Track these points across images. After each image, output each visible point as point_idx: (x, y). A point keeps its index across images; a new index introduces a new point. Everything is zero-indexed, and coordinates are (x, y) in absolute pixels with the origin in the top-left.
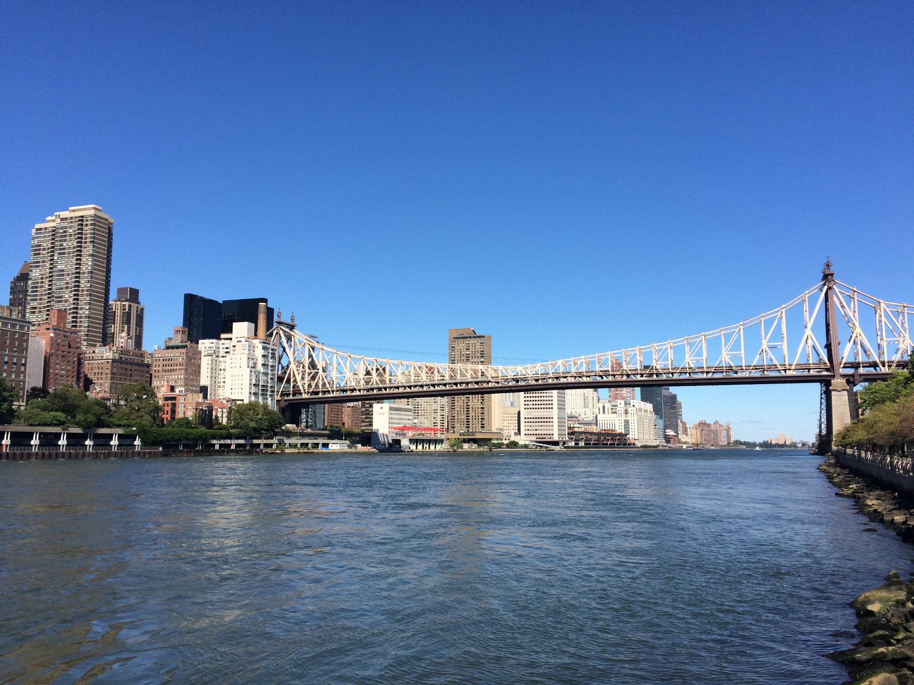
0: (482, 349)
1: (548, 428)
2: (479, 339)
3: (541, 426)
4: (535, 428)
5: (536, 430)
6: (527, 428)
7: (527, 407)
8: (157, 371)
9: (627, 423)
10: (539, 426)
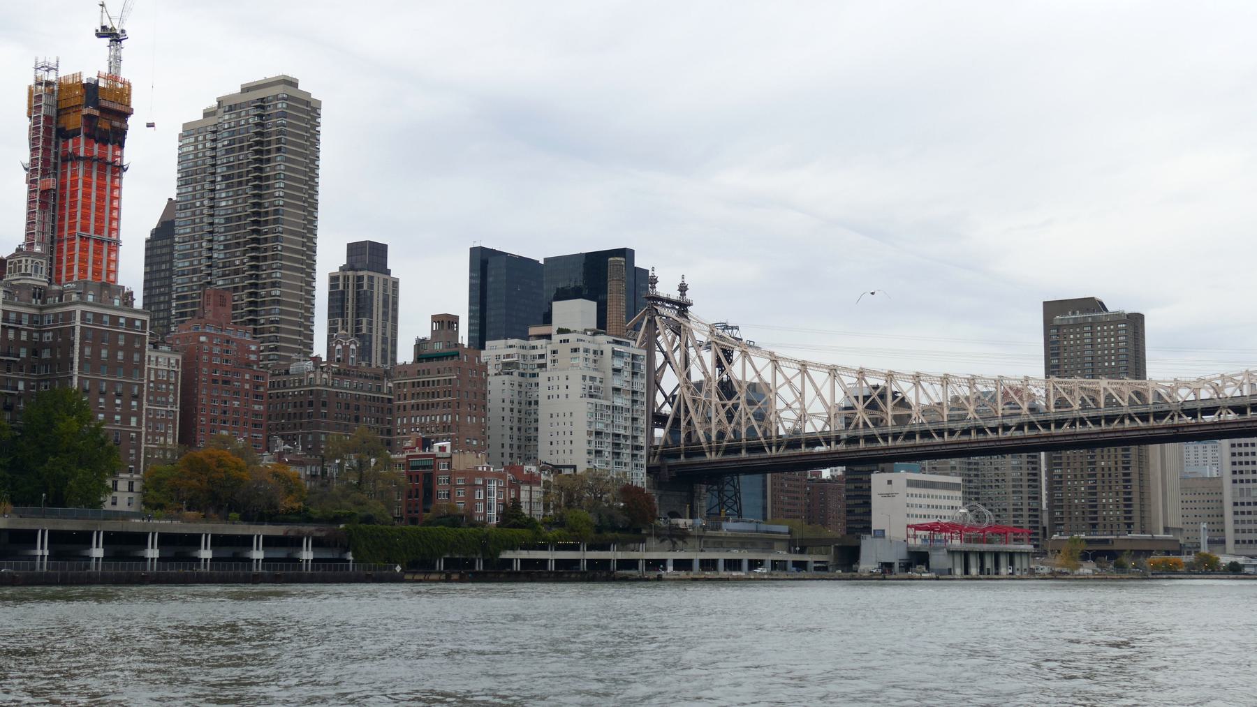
7: (1238, 477)
8: (402, 408)
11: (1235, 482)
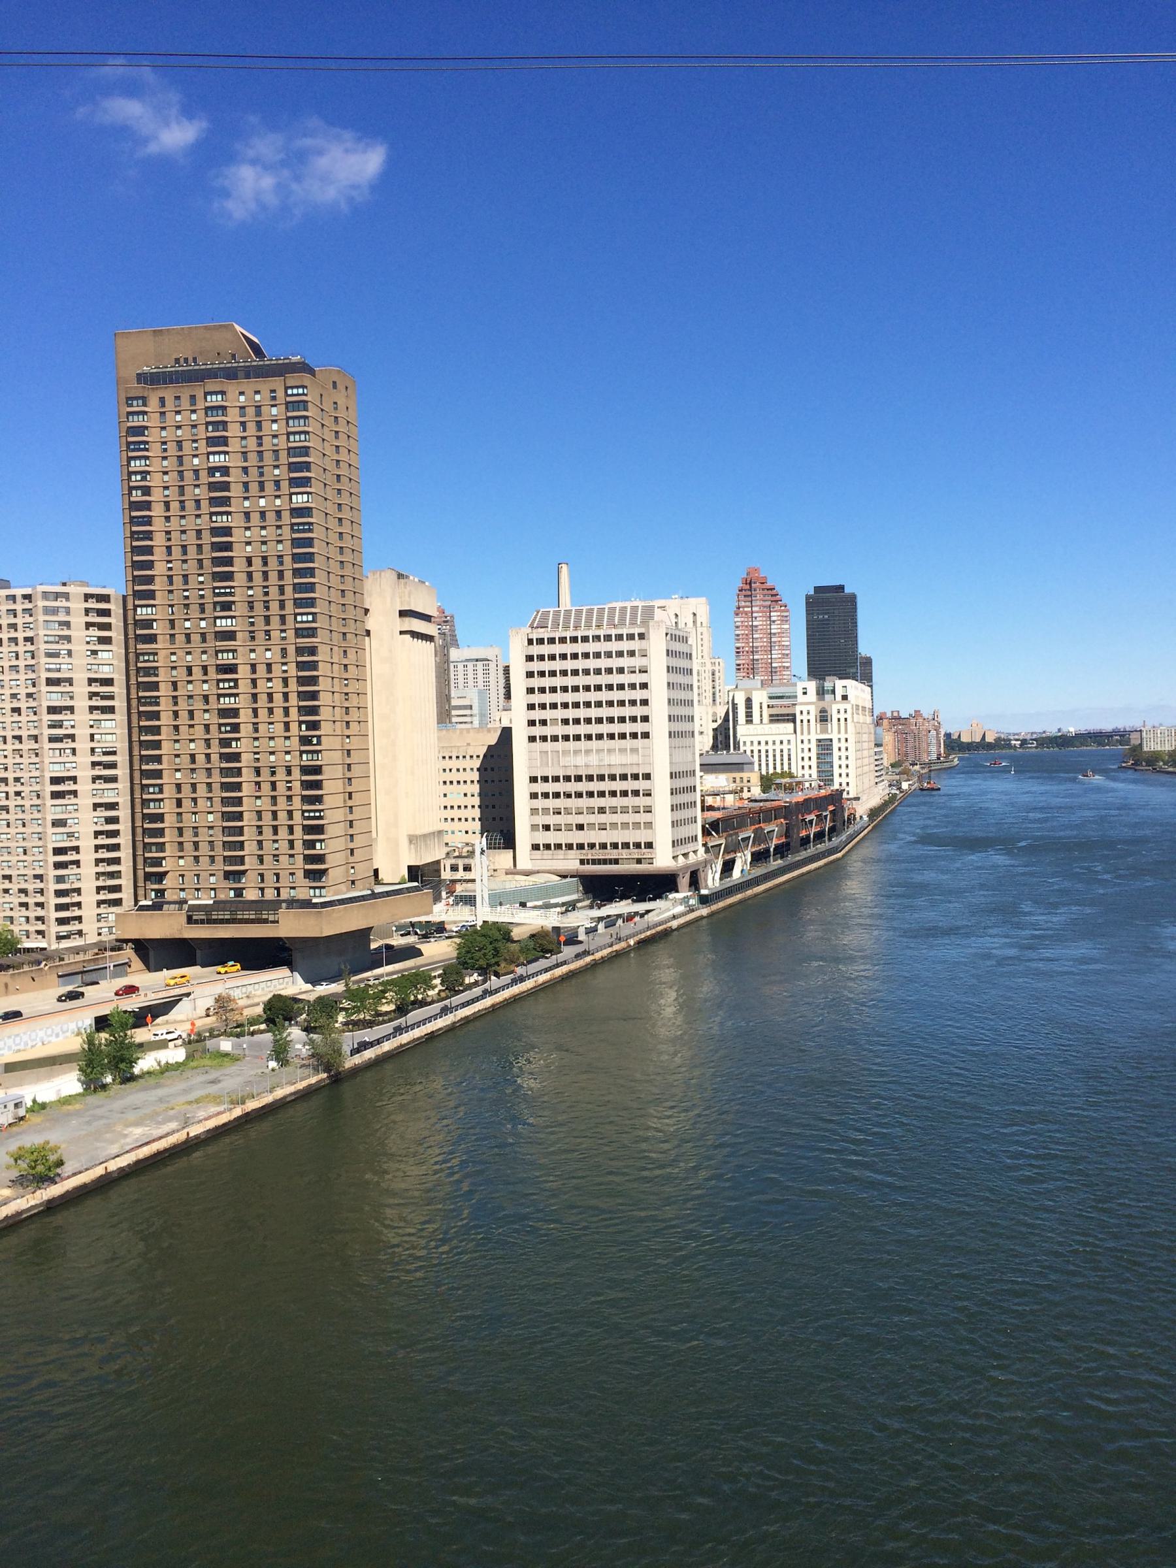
0: (297, 441)
1: (631, 818)
2: (277, 383)
3: (602, 810)
5: (580, 827)
6: (541, 820)
7: (538, 731)
9: (825, 747)
10: (591, 811)
11: (532, 739)
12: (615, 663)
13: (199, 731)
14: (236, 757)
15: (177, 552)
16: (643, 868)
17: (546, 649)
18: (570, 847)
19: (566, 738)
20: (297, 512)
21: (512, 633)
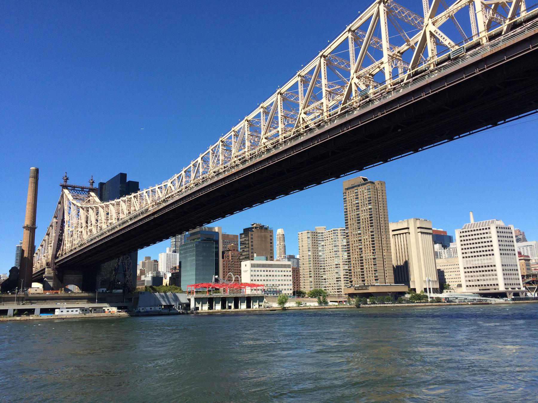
1: (491, 277)
3: (483, 276)
4: (477, 278)
5: (478, 280)
6: (468, 279)
7: (465, 255)
10: (480, 276)
11: (464, 257)
12: (483, 236)
13: (356, 252)
14: (362, 257)
15: (352, 219)
16: (496, 291)
17: (465, 234)
18: (476, 286)
19: (472, 257)
20: (370, 209)
21: (456, 230)
